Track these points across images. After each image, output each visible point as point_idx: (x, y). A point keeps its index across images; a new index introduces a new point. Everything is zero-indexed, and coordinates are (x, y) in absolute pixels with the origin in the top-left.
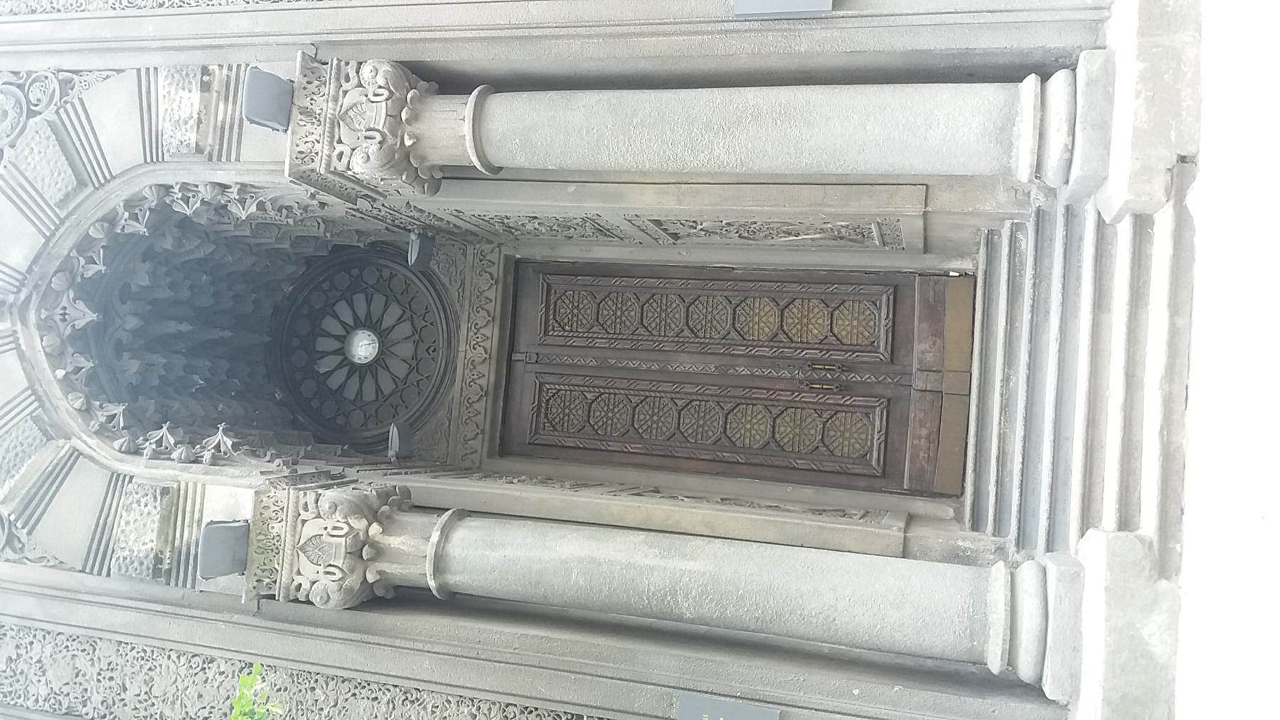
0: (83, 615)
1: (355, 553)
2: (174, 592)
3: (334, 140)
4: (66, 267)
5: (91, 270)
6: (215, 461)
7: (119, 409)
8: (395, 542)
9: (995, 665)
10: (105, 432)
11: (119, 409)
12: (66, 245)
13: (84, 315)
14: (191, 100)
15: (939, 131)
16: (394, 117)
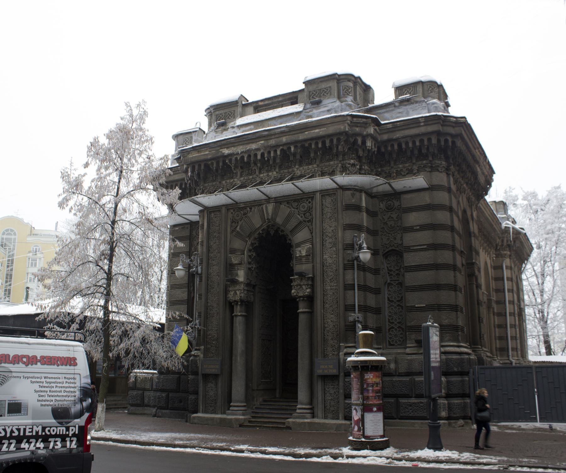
0: (223, 251)
1: (235, 301)
2: (228, 266)
3: (297, 285)
4: (279, 228)
5: (280, 232)
6: (249, 269)
7: (257, 244)
8: (239, 307)
9: (232, 404)
10: (252, 244)
11: (257, 244)
12: (282, 228)
13: (272, 232)
14: (304, 253)
15: (302, 394)
16: (301, 297)
